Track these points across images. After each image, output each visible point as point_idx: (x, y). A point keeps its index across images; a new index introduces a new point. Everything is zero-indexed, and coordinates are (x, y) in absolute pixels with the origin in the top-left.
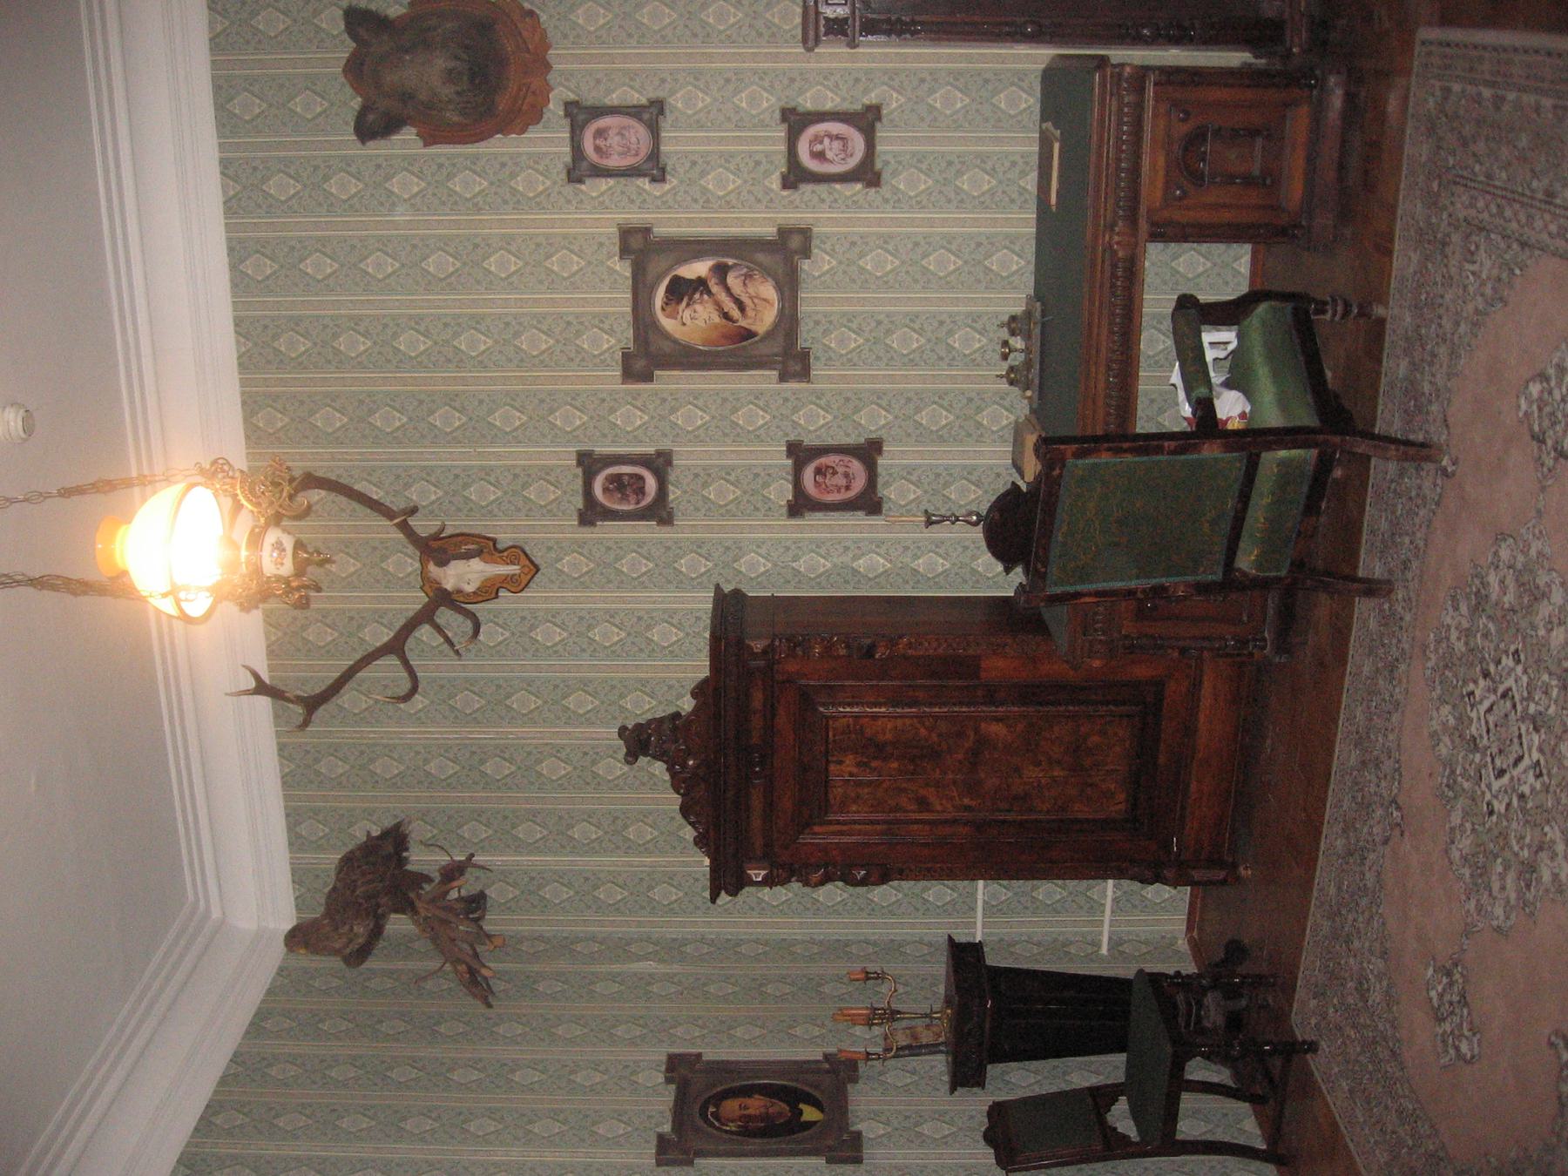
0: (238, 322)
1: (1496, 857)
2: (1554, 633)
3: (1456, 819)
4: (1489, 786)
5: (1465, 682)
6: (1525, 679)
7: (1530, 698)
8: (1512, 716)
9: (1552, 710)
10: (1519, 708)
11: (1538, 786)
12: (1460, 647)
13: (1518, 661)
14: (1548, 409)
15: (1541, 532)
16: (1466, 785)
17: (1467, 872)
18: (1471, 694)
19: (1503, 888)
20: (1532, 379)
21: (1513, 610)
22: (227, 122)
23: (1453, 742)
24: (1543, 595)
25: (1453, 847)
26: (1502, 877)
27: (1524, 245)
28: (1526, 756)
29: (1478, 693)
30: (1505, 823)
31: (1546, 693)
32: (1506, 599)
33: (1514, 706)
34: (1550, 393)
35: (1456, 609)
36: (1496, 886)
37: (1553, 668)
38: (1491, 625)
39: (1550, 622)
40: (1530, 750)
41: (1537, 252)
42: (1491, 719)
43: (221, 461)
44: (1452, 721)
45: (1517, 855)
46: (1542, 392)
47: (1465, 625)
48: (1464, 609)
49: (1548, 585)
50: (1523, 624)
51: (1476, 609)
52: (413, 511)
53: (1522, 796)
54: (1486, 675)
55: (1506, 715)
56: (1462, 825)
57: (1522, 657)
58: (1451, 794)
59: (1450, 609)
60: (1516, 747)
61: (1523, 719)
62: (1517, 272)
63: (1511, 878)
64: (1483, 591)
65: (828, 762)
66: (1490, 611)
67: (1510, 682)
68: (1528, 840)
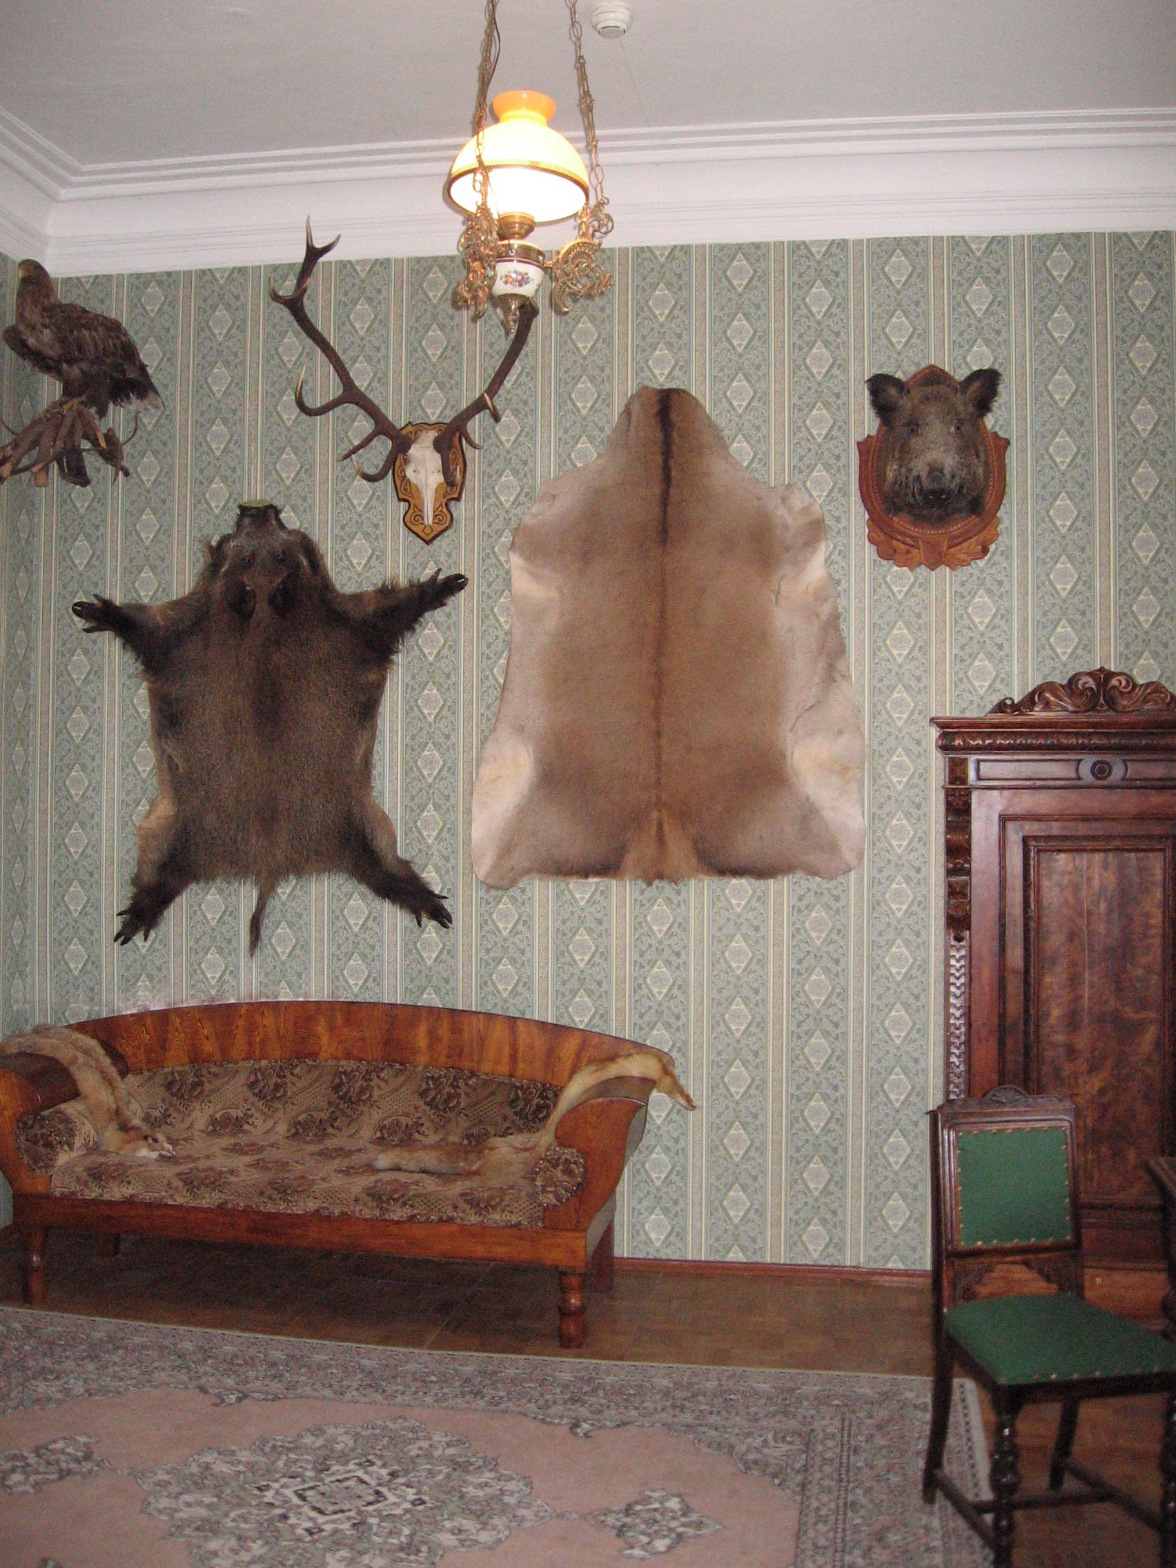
0: (842, 244)
1: (218, 1496)
2: (451, 1537)
3: (244, 1456)
4: (285, 1486)
5: (380, 1457)
6: (399, 1511)
7: (383, 1518)
8: (360, 1503)
9: (375, 1539)
10: (371, 1508)
11: (299, 1531)
12: (413, 1451)
13: (413, 1503)
14: (659, 1517)
15: (543, 1518)
16: (281, 1464)
17: (195, 1469)
18: (373, 1464)
19: (189, 1505)
20: (683, 1501)
21: (462, 1497)
22: (1045, 244)
23: (319, 1448)
24: (485, 1524)
25: (216, 1455)
26: (199, 1503)
27: (803, 1486)
28: (327, 1518)
29: (374, 1468)
30: (254, 1503)
31: (391, 1533)
32: (470, 1489)
33: (370, 1503)
34: (674, 1518)
35: (449, 1445)
36: (187, 1498)
37: (417, 1538)
38: (440, 1477)
39: (460, 1531)
40: (333, 1522)
41: (798, 1498)
42: (351, 1483)
43: (610, 225)
44: (339, 1447)
45: (226, 1515)
46: (672, 1511)
47: (436, 1453)
48: (451, 1451)
49: (494, 1528)
50: (452, 1507)
51: (454, 1463)
52: (496, 417)
53: (284, 1517)
54: (393, 1475)
55: (359, 1497)
56: (239, 1462)
57: (421, 1508)
58: (267, 1449)
59: (448, 1439)
60: (331, 1508)
61: (360, 1512)
62: (777, 1481)
63: (203, 1512)
64: (472, 1468)
65: (1105, 851)
66: (455, 1475)
67: (392, 1498)
68: (243, 1526)
